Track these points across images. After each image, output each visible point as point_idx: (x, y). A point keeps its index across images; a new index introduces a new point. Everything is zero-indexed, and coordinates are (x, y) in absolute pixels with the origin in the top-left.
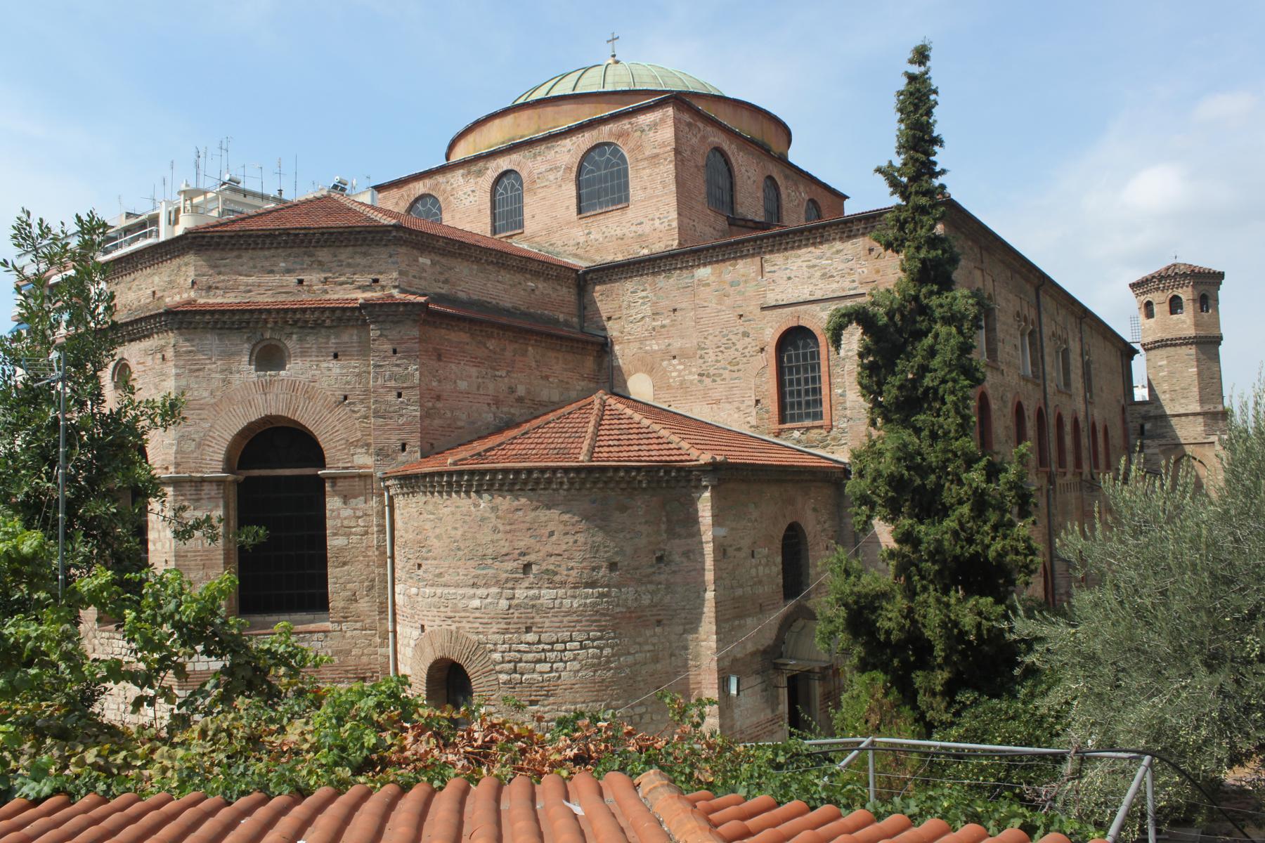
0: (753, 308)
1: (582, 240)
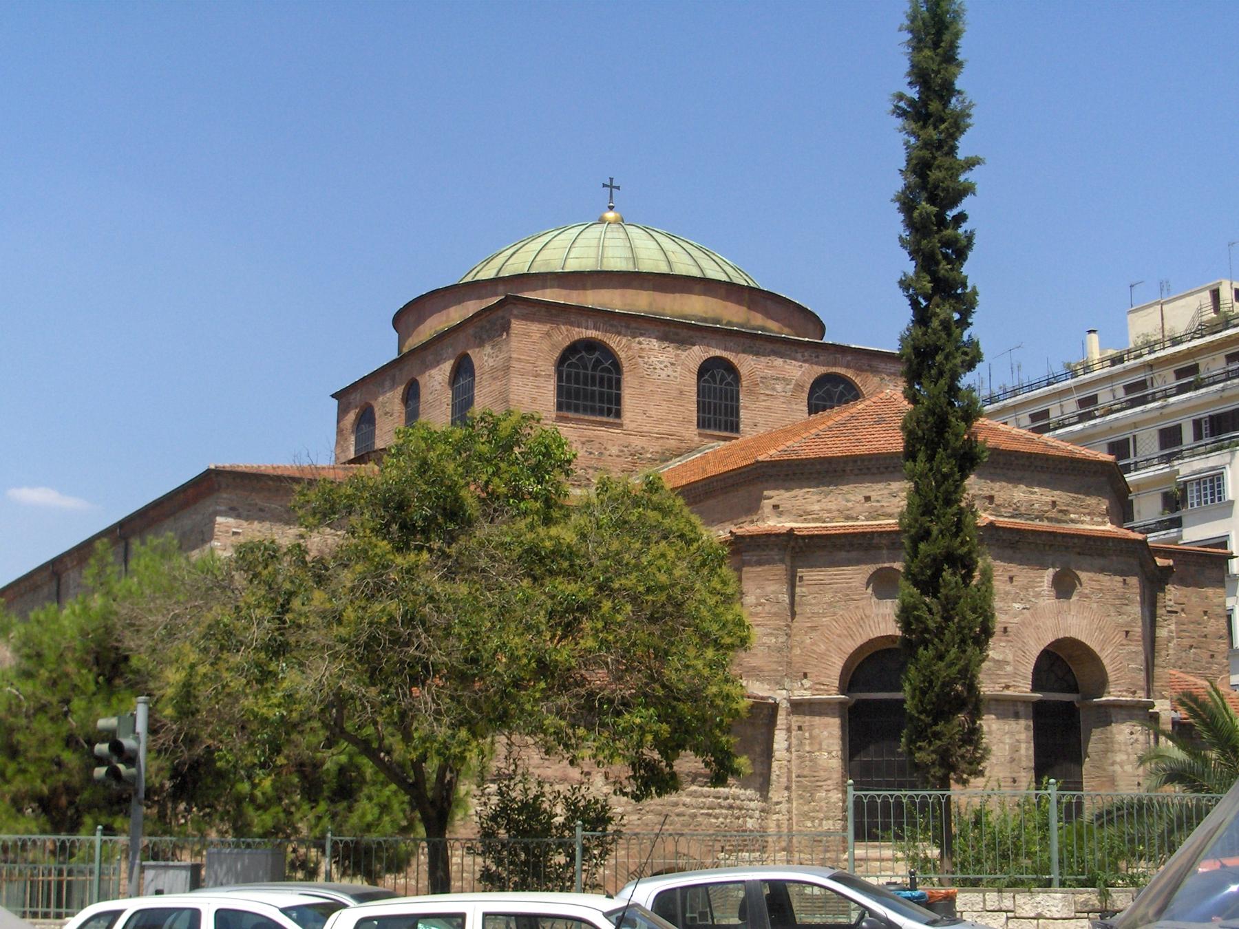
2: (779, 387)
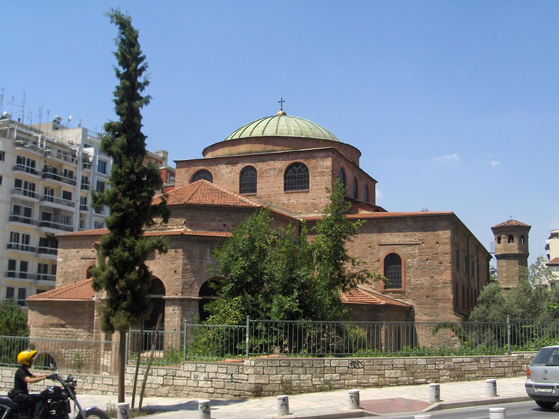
0: (375, 244)
1: (286, 202)
2: (272, 173)
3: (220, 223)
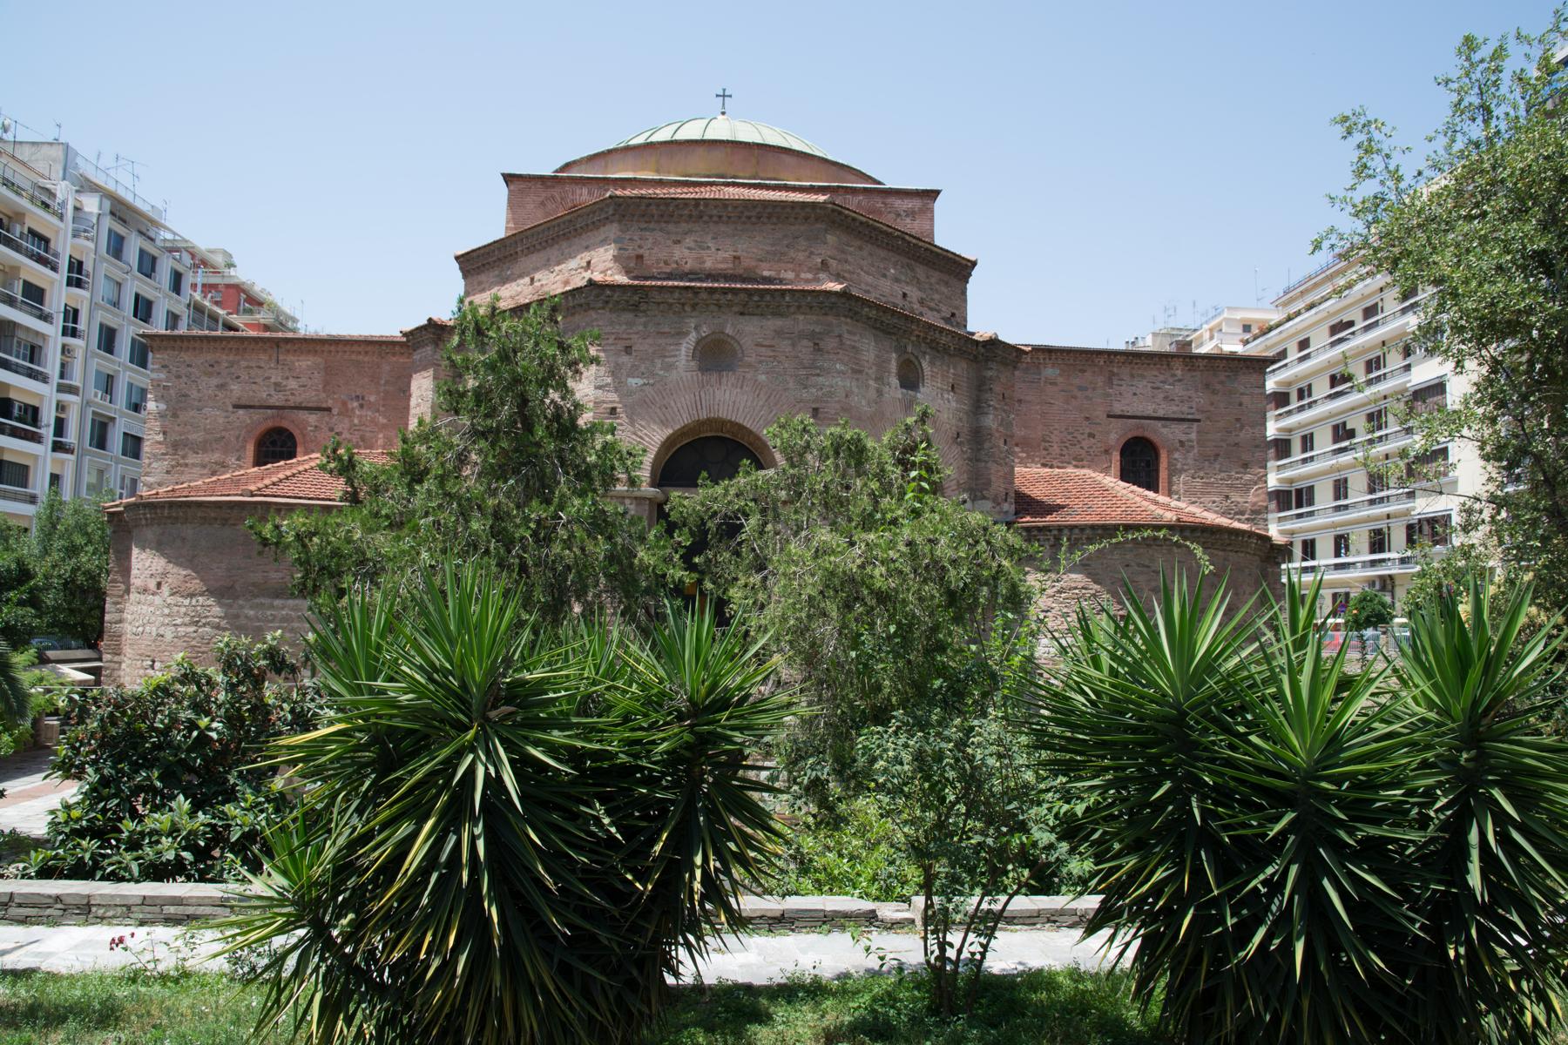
3: (896, 287)
